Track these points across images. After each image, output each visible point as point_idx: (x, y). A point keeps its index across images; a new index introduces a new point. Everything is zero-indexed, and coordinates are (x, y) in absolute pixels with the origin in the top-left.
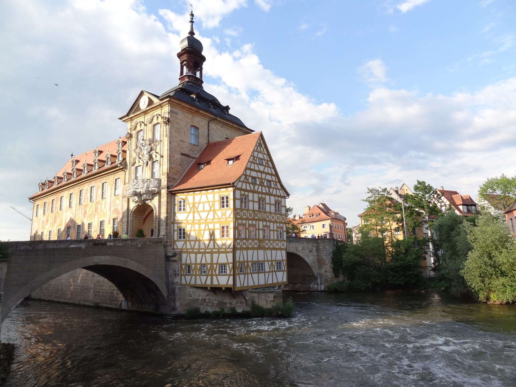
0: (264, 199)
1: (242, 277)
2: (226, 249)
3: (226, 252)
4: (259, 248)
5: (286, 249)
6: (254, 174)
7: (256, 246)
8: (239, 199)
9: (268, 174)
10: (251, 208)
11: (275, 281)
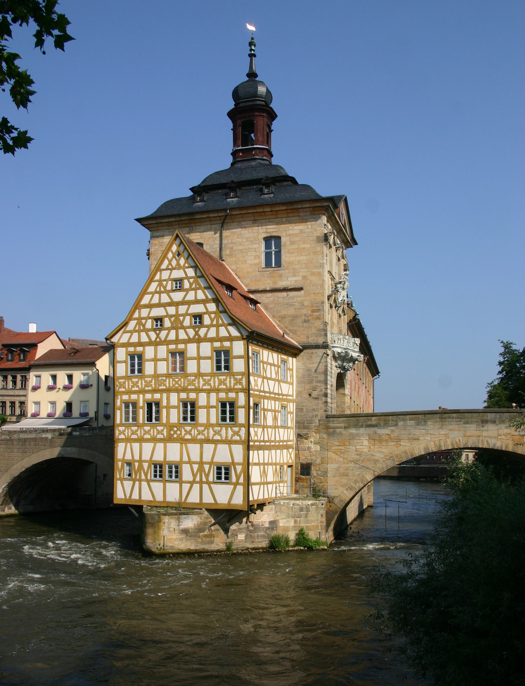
0: (182, 354)
1: (128, 484)
4: (169, 439)
7: (160, 436)
8: (125, 362)
9: (197, 302)
11: (208, 499)
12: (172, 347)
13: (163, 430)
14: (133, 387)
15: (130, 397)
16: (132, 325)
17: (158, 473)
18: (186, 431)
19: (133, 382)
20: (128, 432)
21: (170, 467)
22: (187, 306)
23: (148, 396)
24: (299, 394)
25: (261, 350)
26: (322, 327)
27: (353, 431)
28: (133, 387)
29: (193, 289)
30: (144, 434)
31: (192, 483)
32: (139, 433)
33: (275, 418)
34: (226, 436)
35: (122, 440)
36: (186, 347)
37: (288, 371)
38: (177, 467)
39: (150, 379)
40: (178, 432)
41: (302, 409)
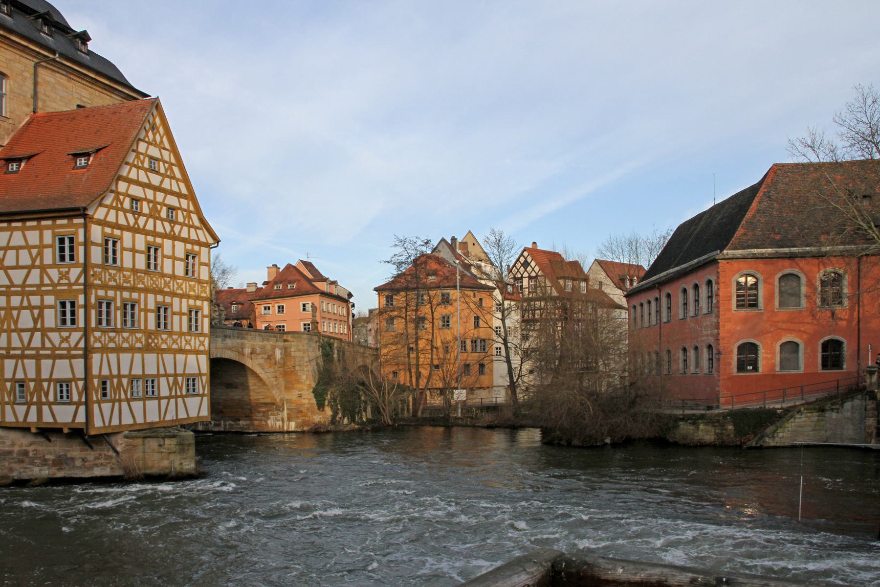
1: (107, 407)
2: (69, 349)
3: (70, 357)
5: (209, 353)
7: (138, 345)
10: (128, 264)
13: (141, 338)
14: (110, 280)
15: (106, 293)
19: (110, 274)
28: (110, 280)
29: (168, 177)
32: (117, 340)
38: (153, 381)
40: (156, 341)
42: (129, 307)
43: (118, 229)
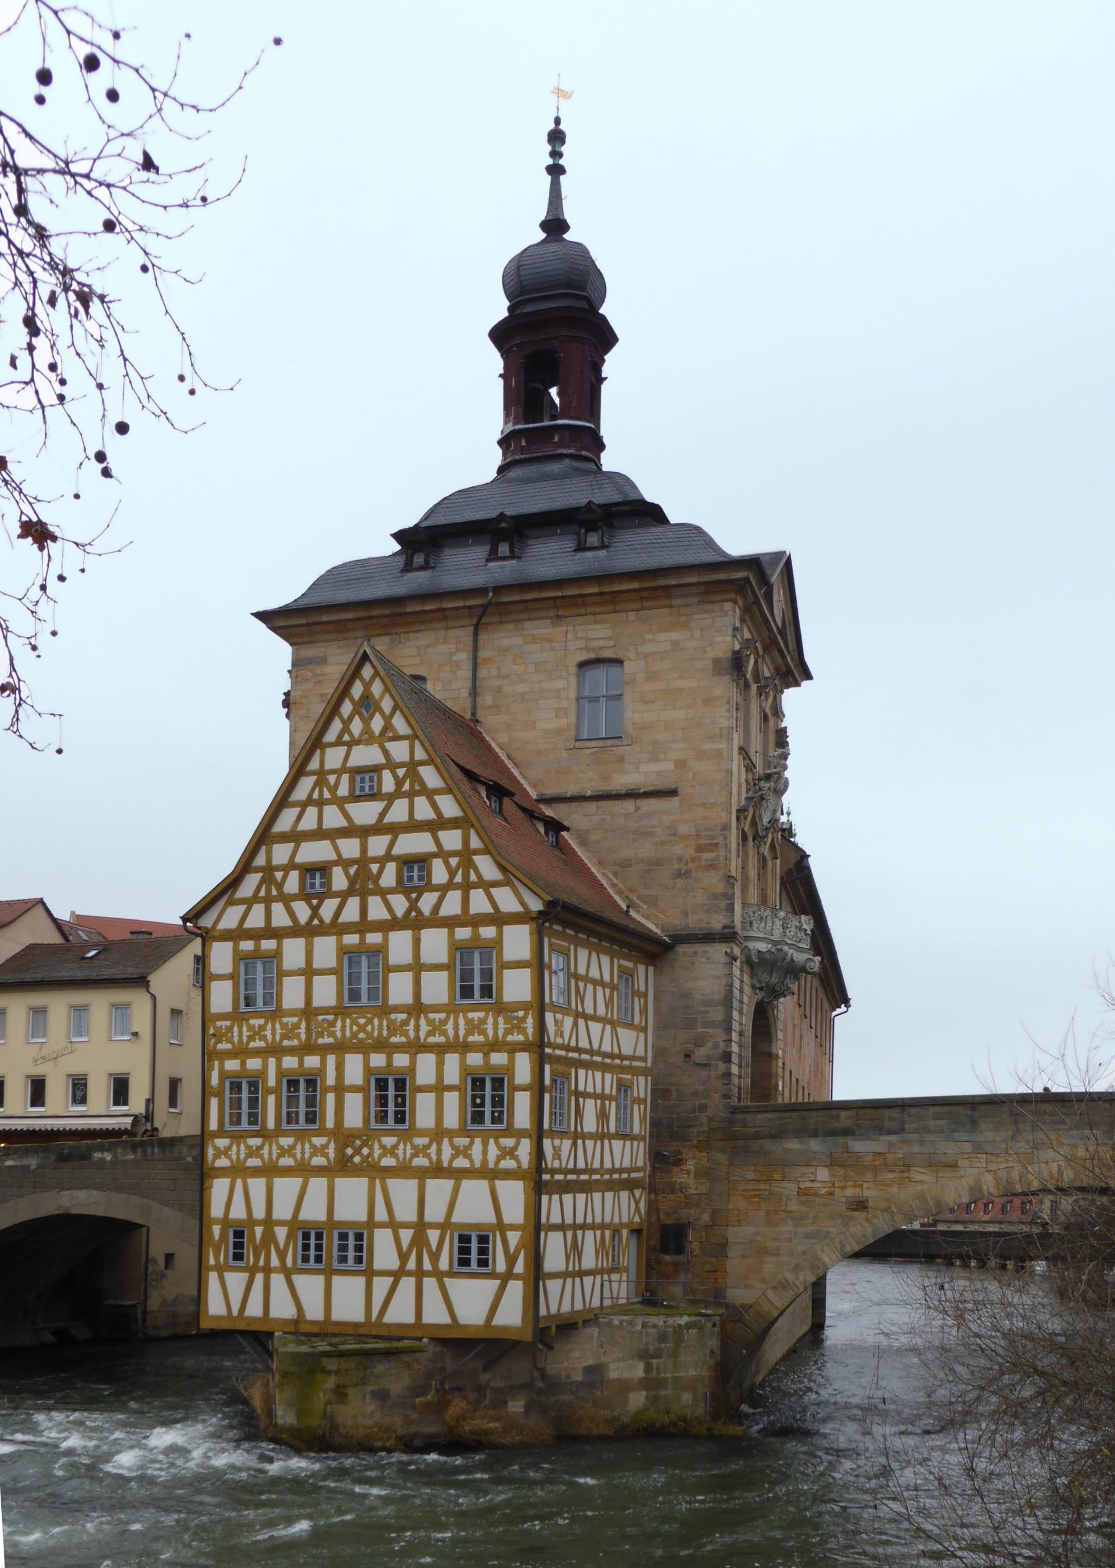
1: (236, 1280)
4: (343, 1167)
6: (314, 852)
7: (318, 1161)
9: (413, 826)
11: (435, 1314)
12: (352, 939)
14: (251, 1038)
15: (243, 1063)
16: (250, 885)
17: (312, 1253)
18: (383, 1147)
19: (251, 1028)
20: (238, 1151)
21: (343, 1237)
22: (388, 837)
23: (290, 1062)
24: (660, 1053)
25: (572, 947)
26: (720, 888)
27: (794, 1145)
28: (251, 1038)
30: (280, 1156)
31: (397, 1275)
32: (265, 1151)
33: (603, 1116)
34: (485, 1161)
35: (222, 1172)
36: (386, 940)
37: (636, 999)
38: (359, 1237)
39: (295, 1020)
40: (365, 1151)
41: (667, 1092)
42: (304, 1088)
43: (270, 938)
